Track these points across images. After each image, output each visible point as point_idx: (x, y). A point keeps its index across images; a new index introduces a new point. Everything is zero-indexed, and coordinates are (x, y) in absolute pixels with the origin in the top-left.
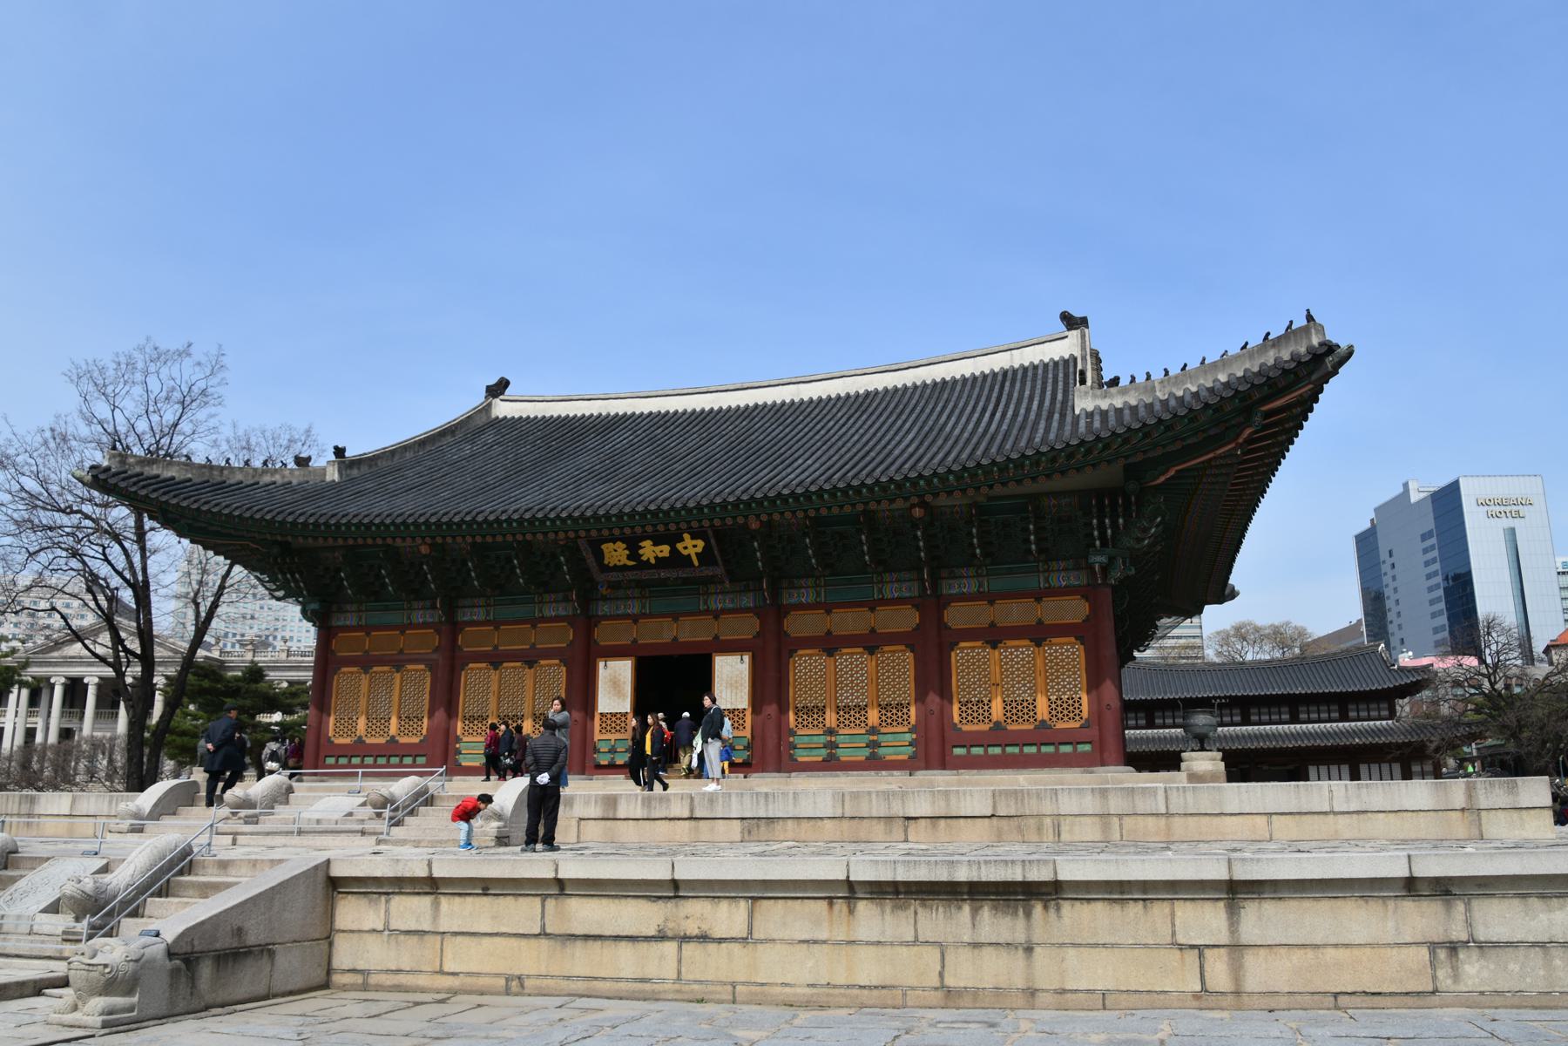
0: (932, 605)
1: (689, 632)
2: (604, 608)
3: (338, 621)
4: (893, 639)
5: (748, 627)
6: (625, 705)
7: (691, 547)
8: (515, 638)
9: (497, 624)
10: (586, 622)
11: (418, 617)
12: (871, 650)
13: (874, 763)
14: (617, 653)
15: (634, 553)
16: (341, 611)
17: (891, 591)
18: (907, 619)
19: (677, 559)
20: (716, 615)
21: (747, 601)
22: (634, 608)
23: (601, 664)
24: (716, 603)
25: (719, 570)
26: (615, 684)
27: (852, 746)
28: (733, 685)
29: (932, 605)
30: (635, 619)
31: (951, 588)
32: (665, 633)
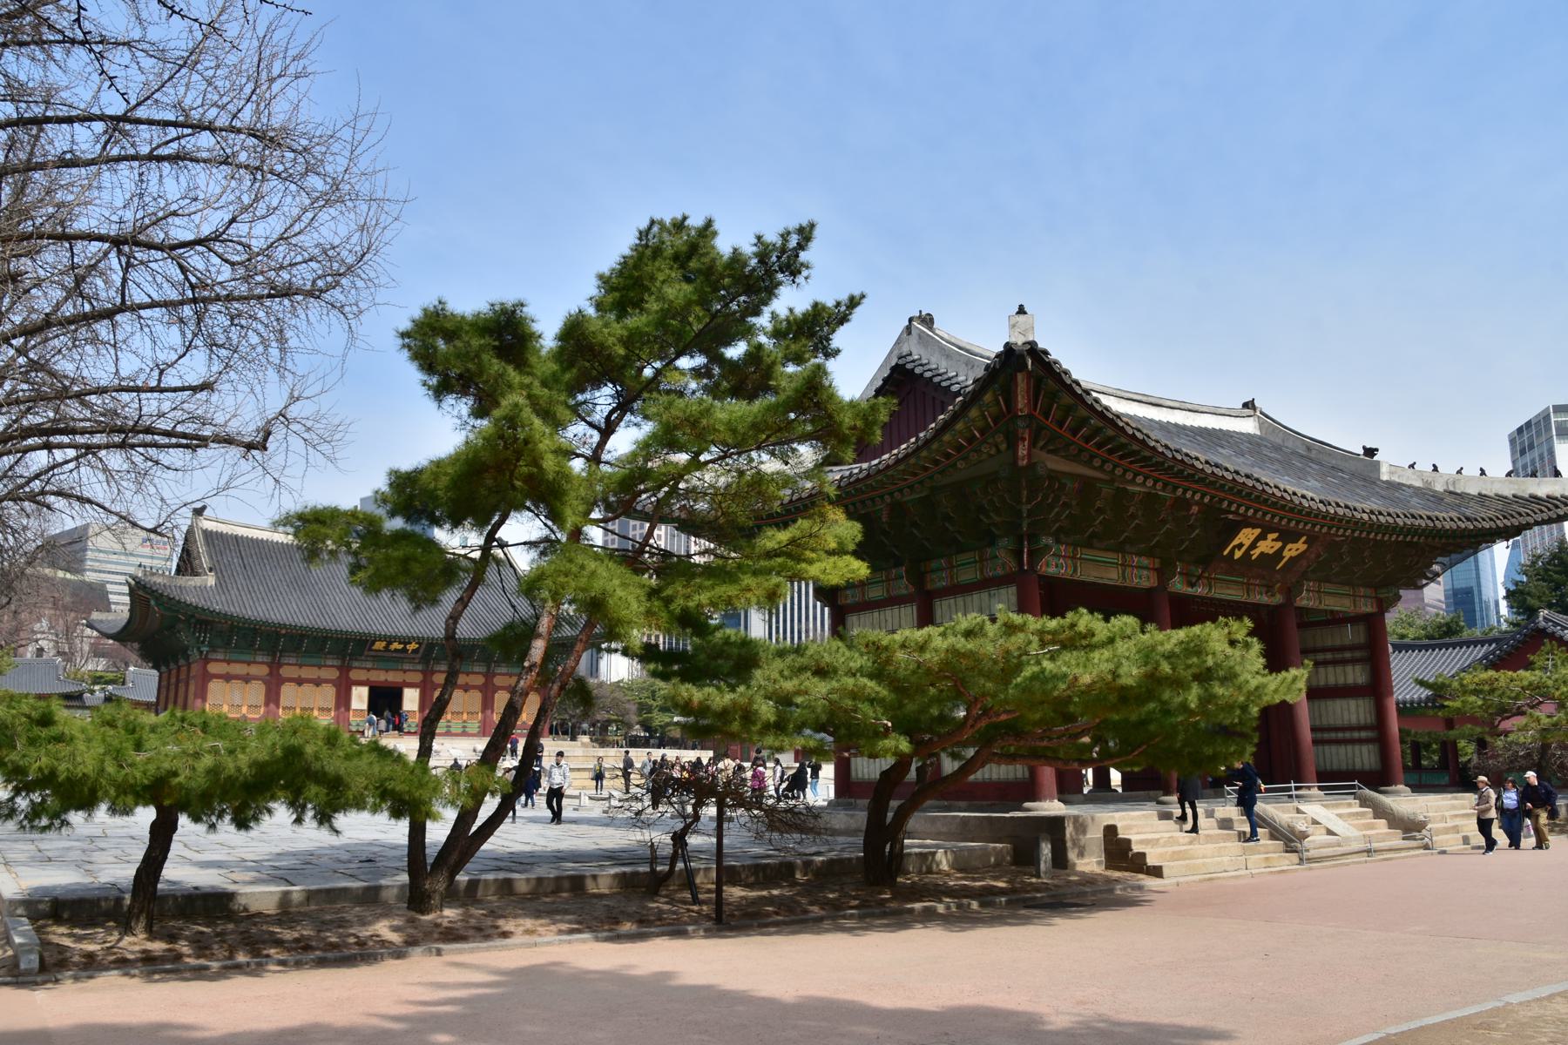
0: (489, 676)
1: (392, 677)
2: (356, 664)
3: (211, 656)
4: (474, 687)
5: (418, 677)
6: (365, 706)
7: (413, 646)
8: (306, 673)
9: (301, 666)
10: (344, 670)
11: (259, 659)
12: (466, 691)
13: (464, 734)
14: (360, 683)
15: (387, 648)
16: (215, 651)
17: (477, 669)
18: (480, 680)
19: (404, 650)
20: (405, 671)
21: (419, 667)
22: (369, 665)
23: (354, 688)
24: (406, 667)
25: (419, 655)
26: (360, 696)
27: (456, 729)
28: (412, 701)
29: (489, 676)
30: (369, 670)
31: (499, 670)
32: (381, 677)
